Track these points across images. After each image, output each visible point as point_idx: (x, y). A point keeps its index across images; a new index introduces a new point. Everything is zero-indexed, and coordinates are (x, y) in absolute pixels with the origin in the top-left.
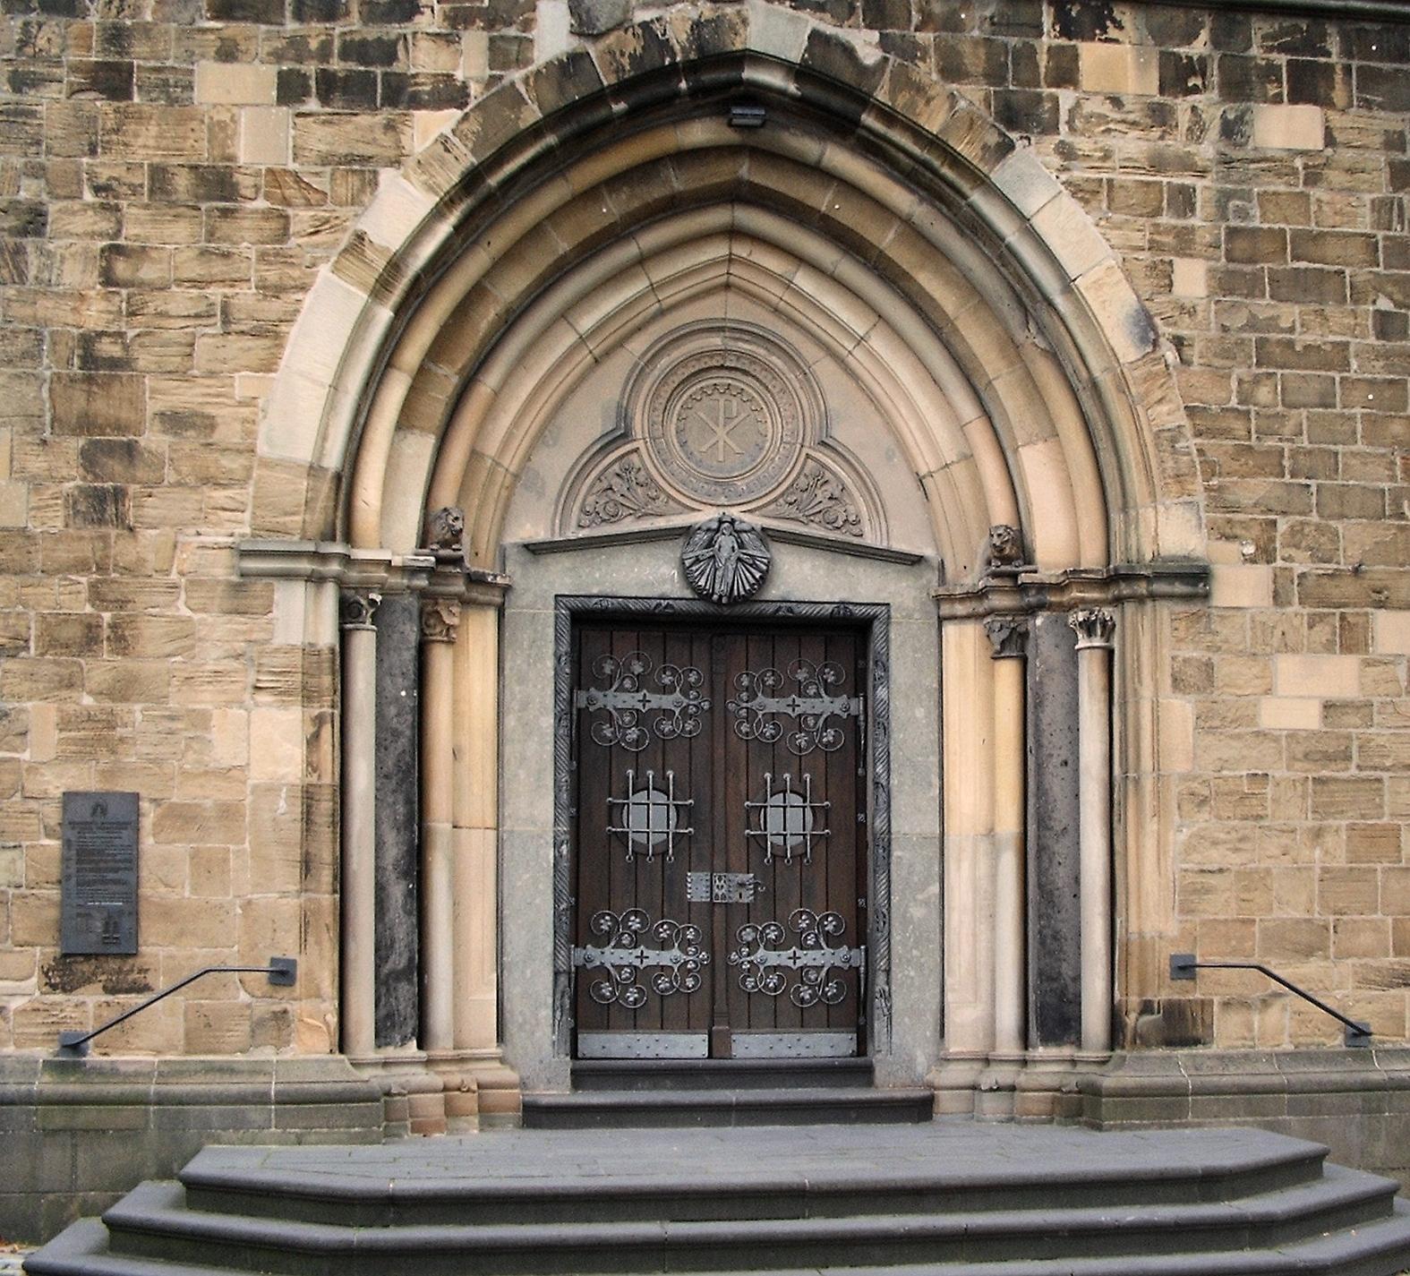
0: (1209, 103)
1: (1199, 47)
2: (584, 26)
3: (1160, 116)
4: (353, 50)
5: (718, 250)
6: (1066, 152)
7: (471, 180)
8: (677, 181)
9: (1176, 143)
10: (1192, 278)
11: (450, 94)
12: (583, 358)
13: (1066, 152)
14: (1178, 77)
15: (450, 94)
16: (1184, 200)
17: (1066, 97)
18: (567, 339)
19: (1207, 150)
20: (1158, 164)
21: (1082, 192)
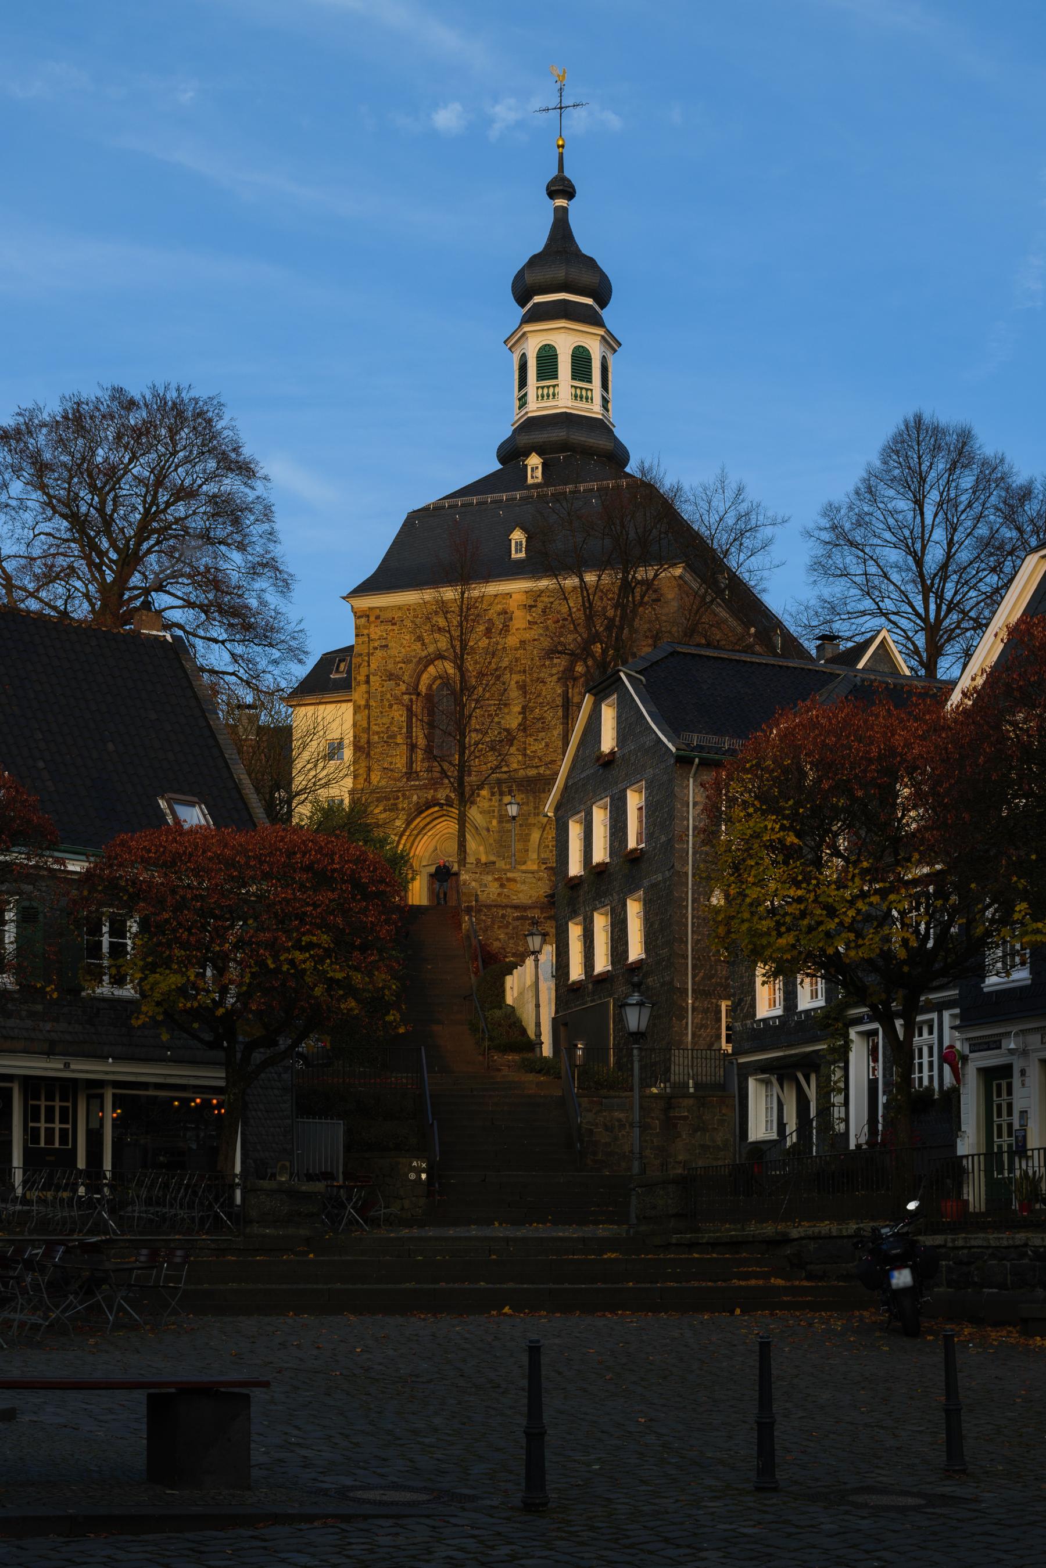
0: (497, 797)
1: (496, 789)
2: (419, 798)
3: (491, 800)
4: (392, 805)
5: (446, 823)
6: (478, 807)
7: (406, 820)
8: (436, 815)
9: (493, 803)
10: (495, 822)
11: (403, 809)
12: (429, 840)
13: (478, 807)
14: (493, 794)
15: (403, 809)
16: (494, 811)
17: (478, 799)
18: (426, 837)
19: (497, 804)
20: (490, 806)
21: (481, 813)
